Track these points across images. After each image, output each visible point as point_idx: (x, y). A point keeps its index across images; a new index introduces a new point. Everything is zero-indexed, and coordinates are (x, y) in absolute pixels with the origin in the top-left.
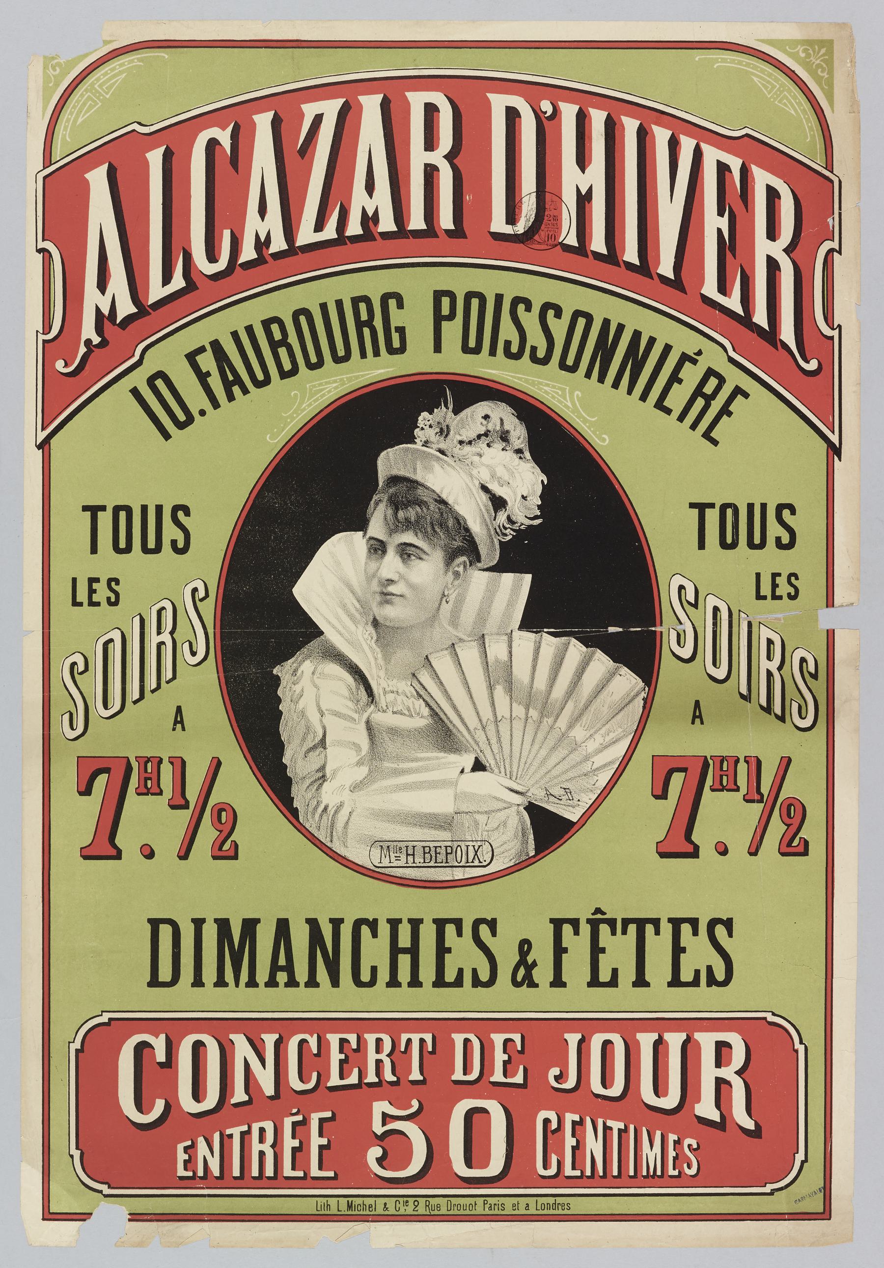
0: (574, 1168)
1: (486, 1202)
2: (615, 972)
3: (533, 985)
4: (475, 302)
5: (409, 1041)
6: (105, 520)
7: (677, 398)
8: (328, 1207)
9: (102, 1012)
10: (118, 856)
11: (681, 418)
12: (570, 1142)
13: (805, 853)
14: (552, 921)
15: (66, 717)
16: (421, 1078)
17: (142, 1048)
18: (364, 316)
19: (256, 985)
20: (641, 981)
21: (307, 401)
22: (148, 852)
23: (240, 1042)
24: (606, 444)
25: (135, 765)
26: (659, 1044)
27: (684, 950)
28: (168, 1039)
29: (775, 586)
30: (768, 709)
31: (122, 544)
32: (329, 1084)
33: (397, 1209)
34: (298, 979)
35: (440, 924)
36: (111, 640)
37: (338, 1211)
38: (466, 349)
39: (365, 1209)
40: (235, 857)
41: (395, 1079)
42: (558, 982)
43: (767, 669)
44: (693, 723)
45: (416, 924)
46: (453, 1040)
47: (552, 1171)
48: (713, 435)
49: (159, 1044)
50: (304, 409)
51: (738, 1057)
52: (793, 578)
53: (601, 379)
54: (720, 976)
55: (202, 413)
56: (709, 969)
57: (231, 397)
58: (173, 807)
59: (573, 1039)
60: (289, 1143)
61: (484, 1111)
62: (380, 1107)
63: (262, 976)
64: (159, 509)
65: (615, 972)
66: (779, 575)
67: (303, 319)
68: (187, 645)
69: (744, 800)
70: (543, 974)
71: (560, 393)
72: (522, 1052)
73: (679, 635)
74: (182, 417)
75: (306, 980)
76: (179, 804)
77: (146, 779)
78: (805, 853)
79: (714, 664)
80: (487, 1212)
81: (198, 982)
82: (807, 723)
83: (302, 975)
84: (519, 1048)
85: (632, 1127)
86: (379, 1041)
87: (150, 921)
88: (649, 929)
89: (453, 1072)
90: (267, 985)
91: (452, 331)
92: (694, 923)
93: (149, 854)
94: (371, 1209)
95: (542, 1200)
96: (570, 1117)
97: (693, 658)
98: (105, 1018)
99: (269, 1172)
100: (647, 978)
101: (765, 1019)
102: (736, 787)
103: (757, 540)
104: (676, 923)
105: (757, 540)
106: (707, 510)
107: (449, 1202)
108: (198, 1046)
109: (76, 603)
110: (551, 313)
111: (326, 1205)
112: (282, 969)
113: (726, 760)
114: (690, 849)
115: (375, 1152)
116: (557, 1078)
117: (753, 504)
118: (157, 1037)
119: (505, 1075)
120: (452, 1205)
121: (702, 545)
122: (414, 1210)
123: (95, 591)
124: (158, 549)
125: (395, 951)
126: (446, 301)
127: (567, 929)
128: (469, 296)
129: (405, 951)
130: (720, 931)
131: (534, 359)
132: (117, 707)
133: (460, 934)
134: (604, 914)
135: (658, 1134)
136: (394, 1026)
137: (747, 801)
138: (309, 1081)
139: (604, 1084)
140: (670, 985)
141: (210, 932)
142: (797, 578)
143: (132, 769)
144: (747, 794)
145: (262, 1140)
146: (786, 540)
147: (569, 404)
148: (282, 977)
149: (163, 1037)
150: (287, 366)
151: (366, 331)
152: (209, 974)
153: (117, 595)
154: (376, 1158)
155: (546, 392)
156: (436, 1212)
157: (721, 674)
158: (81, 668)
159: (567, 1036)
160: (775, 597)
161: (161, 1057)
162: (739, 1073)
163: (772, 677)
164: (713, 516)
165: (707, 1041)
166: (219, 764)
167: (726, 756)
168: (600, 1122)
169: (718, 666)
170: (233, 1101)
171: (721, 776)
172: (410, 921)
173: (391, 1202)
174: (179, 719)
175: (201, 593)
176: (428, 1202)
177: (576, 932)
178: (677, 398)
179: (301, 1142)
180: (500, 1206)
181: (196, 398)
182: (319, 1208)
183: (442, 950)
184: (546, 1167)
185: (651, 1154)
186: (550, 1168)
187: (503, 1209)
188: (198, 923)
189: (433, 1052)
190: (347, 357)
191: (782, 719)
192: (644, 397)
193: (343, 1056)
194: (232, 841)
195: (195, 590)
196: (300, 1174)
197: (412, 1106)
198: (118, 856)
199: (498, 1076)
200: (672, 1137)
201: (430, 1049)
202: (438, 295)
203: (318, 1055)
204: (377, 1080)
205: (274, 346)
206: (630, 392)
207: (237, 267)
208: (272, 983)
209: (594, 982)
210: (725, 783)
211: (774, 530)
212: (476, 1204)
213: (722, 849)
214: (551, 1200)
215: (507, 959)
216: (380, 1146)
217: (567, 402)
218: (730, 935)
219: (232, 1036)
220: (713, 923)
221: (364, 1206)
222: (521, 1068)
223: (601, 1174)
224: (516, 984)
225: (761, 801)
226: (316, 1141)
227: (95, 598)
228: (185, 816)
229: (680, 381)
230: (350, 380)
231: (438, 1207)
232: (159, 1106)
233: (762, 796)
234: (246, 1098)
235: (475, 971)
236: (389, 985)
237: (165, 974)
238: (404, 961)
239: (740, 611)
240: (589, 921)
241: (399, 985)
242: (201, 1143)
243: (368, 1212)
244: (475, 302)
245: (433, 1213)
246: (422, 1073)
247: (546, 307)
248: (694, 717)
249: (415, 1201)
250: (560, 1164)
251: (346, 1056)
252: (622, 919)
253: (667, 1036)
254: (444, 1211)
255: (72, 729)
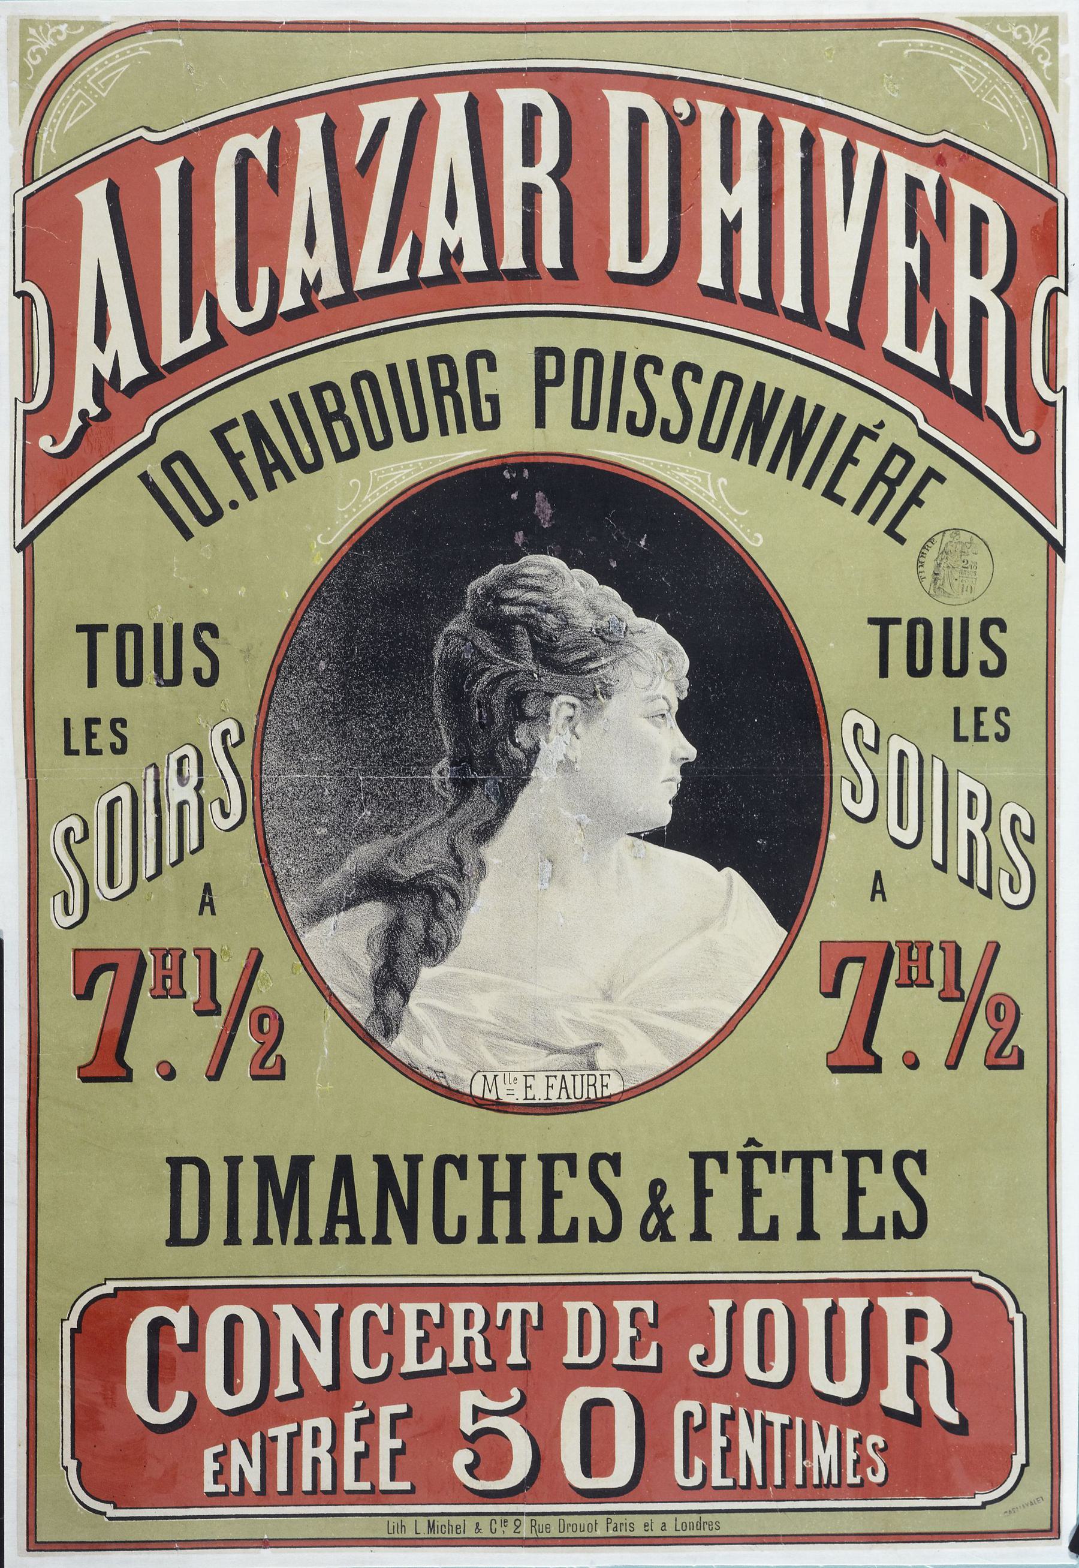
0: (724, 1476)
1: (609, 1521)
2: (774, 1220)
3: (668, 1237)
4: (589, 363)
5: (508, 1313)
6: (106, 643)
7: (852, 484)
8: (403, 1528)
9: (106, 1279)
10: (128, 1076)
11: (857, 509)
12: (718, 1441)
13: (1020, 1065)
14: (692, 1155)
15: (59, 899)
16: (523, 1361)
17: (159, 1328)
18: (445, 382)
19: (309, 1242)
20: (808, 1233)
21: (373, 490)
22: (166, 1071)
23: (287, 1316)
24: (759, 545)
25: (149, 958)
26: (833, 1314)
27: (863, 1192)
28: (192, 1312)
29: (978, 724)
30: (969, 882)
31: (130, 675)
32: (404, 1370)
33: (493, 1531)
34: (363, 1233)
35: (548, 1161)
36: (118, 799)
37: (416, 1533)
38: (577, 423)
39: (450, 1531)
40: (282, 1076)
41: (489, 1362)
42: (700, 1234)
43: (968, 830)
44: (873, 899)
45: (516, 1161)
46: (564, 1310)
47: (696, 1479)
48: (899, 530)
49: (180, 1320)
50: (367, 502)
51: (936, 1330)
52: (1002, 714)
53: (753, 460)
54: (911, 1225)
55: (234, 505)
56: (897, 1216)
57: (271, 485)
58: (200, 1013)
59: (721, 1307)
60: (352, 1446)
61: (607, 1403)
62: (470, 1398)
63: (317, 1227)
64: (178, 629)
65: (774, 1220)
66: (985, 709)
67: (364, 385)
68: (216, 804)
69: (940, 997)
70: (681, 1223)
71: (700, 480)
72: (655, 1325)
73: (854, 788)
74: (207, 511)
75: (374, 1234)
76: (208, 1008)
77: (165, 977)
78: (1020, 1065)
79: (900, 824)
80: (611, 1533)
81: (233, 1238)
82: (1021, 898)
83: (368, 1227)
84: (651, 1320)
85: (799, 1421)
86: (468, 1314)
87: (169, 1160)
88: (818, 1164)
89: (565, 1352)
90: (324, 1241)
91: (559, 399)
92: (876, 1156)
93: (170, 1075)
94: (459, 1531)
95: (682, 1518)
96: (718, 1409)
97: (872, 817)
98: (109, 1288)
99: (326, 1484)
100: (816, 1229)
101: (970, 1279)
102: (928, 982)
103: (956, 665)
104: (853, 1157)
105: (956, 665)
106: (891, 626)
107: (562, 1521)
108: (232, 1324)
109: (69, 751)
110: (688, 376)
111: (400, 1524)
112: (342, 1220)
113: (916, 947)
114: (870, 1061)
115: (463, 1457)
116: (701, 1359)
117: (951, 619)
118: (177, 1310)
119: (633, 1356)
120: (566, 1526)
121: (884, 672)
122: (514, 1532)
123: (95, 736)
124: (176, 680)
125: (490, 1196)
126: (551, 362)
127: (712, 1165)
128: (581, 354)
129: (502, 1196)
130: (910, 1167)
131: (666, 435)
132: (126, 885)
133: (573, 1173)
134: (760, 1145)
135: (833, 1430)
136: (490, 1294)
137: (944, 999)
138: (377, 1364)
139: (763, 1366)
140: (846, 1236)
141: (248, 1174)
142: (1007, 714)
143: (145, 964)
144: (943, 990)
145: (316, 1443)
146: (993, 664)
147: (711, 494)
148: (342, 1231)
149: (185, 1310)
150: (345, 445)
151: (448, 401)
152: (248, 1229)
153: (124, 739)
154: (465, 1465)
155: (683, 480)
156: (544, 1535)
157: (909, 837)
158: (79, 835)
159: (713, 1303)
160: (979, 738)
161: (182, 1336)
162: (937, 1350)
163: (974, 841)
164: (898, 635)
165: (895, 1308)
166: (260, 956)
167: (916, 942)
168: (757, 1415)
169: (904, 827)
170: (278, 1392)
171: (910, 969)
172: (509, 1157)
173: (485, 1521)
174: (207, 902)
175: (234, 737)
176: (533, 1522)
177: (724, 1169)
178: (852, 484)
179: (367, 1446)
180: (628, 1525)
181: (225, 486)
182: (391, 1531)
183: (550, 1195)
184: (687, 1473)
185: (824, 1456)
186: (693, 1475)
187: (632, 1529)
188: (233, 1163)
189: (540, 1327)
190: (423, 434)
191: (988, 893)
192: (808, 483)
193: (421, 1334)
194: (277, 1056)
195: (226, 733)
196: (366, 1486)
197: (510, 1397)
198: (128, 1077)
199: (623, 1357)
200: (851, 1434)
201: (535, 1323)
202: (541, 353)
203: (390, 1332)
204: (466, 1364)
205: (328, 419)
206: (790, 476)
207: (279, 319)
208: (329, 1238)
209: (748, 1233)
210: (914, 976)
211: (978, 651)
212: (596, 1524)
213: (912, 1061)
214: (695, 1518)
215: (634, 1206)
216: (470, 1449)
217: (709, 491)
218: (923, 1172)
219: (277, 1308)
220: (900, 1157)
221: (450, 1527)
222: (654, 1345)
223: (760, 1483)
224: (646, 1237)
225: (961, 999)
226: (387, 1444)
227: (95, 744)
228: (216, 1023)
229: (855, 462)
230: (426, 464)
231: (548, 1527)
232: (180, 1401)
233: (962, 992)
234: (295, 1389)
235: (592, 1221)
236: (481, 1240)
237: (189, 1228)
238: (502, 1208)
239: (933, 756)
240: (740, 1155)
241: (495, 1240)
242: (236, 1446)
243: (455, 1535)
244: (589, 363)
245: (540, 1535)
246: (524, 1355)
247: (682, 368)
248: (875, 892)
249: (516, 1520)
250: (706, 1470)
251: (426, 1333)
252: (783, 1152)
253: (843, 1302)
254: (555, 1533)
255: (67, 913)
